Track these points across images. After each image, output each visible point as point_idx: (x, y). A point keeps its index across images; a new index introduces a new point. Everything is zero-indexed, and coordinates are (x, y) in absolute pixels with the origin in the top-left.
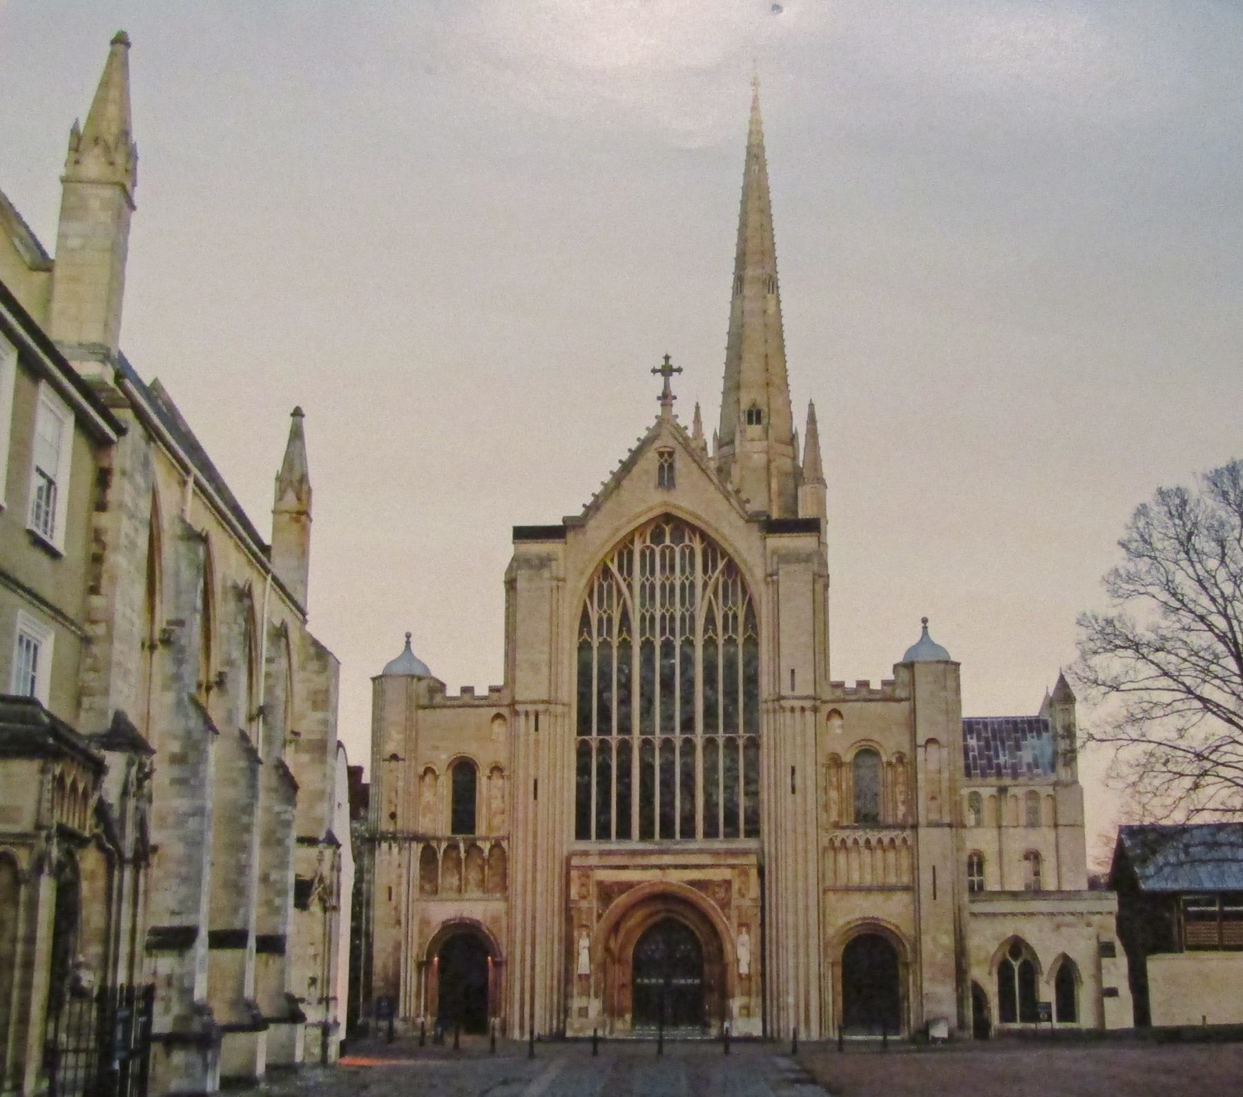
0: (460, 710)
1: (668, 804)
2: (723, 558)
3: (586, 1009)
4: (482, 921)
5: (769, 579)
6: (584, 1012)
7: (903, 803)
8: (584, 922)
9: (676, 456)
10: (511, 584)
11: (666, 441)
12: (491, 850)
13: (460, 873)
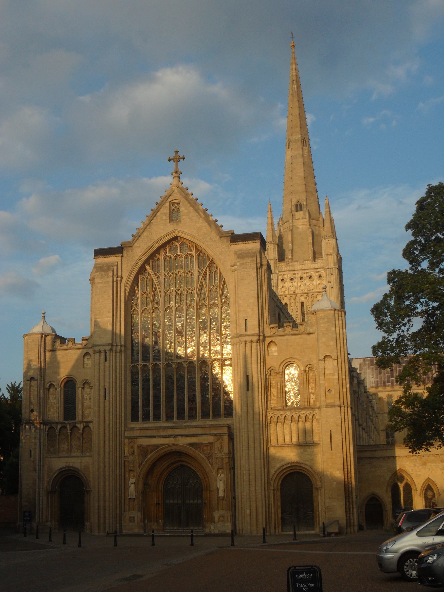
0: (68, 351)
1: (181, 401)
2: (209, 259)
3: (134, 518)
4: (79, 467)
5: (233, 268)
6: (132, 520)
7: (313, 394)
8: (132, 469)
9: (181, 205)
10: (92, 280)
11: (177, 196)
12: (83, 429)
13: (68, 442)
